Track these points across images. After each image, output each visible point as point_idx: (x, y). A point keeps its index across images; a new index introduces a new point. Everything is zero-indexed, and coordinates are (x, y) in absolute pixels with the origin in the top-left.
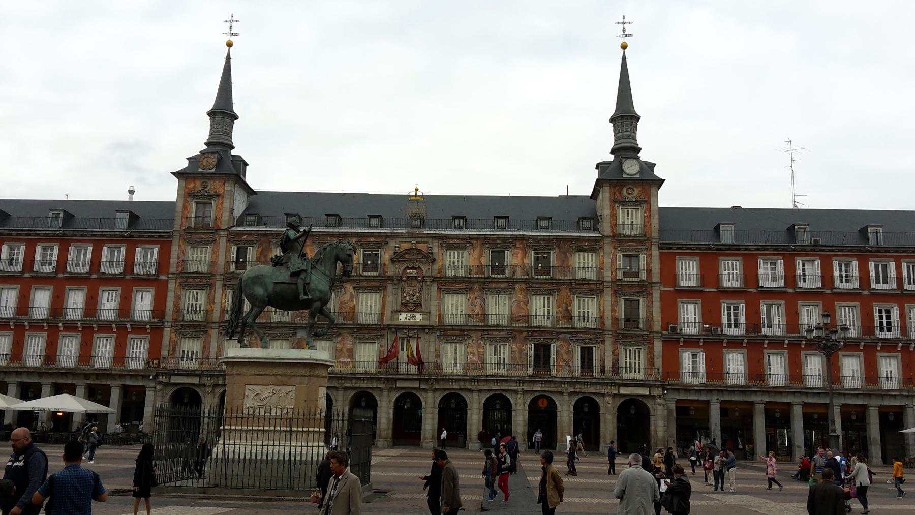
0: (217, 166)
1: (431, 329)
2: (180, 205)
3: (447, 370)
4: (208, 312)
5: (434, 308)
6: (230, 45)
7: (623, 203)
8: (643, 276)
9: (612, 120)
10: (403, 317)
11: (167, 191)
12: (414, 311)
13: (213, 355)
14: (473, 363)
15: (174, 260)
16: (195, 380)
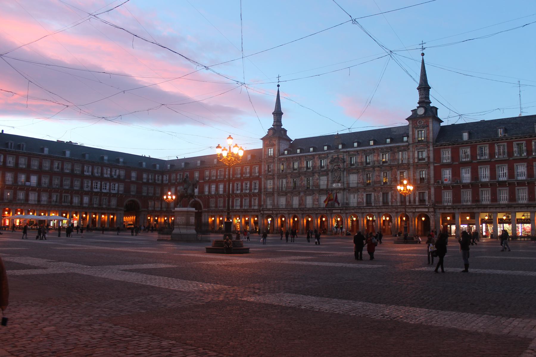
0: (277, 133)
1: (344, 189)
2: (263, 150)
3: (351, 205)
4: (273, 188)
5: (345, 180)
6: (278, 86)
7: (417, 128)
8: (426, 160)
9: (418, 89)
10: (334, 185)
11: (259, 145)
12: (338, 182)
13: (276, 204)
14: (360, 202)
15: (263, 170)
16: (271, 212)
